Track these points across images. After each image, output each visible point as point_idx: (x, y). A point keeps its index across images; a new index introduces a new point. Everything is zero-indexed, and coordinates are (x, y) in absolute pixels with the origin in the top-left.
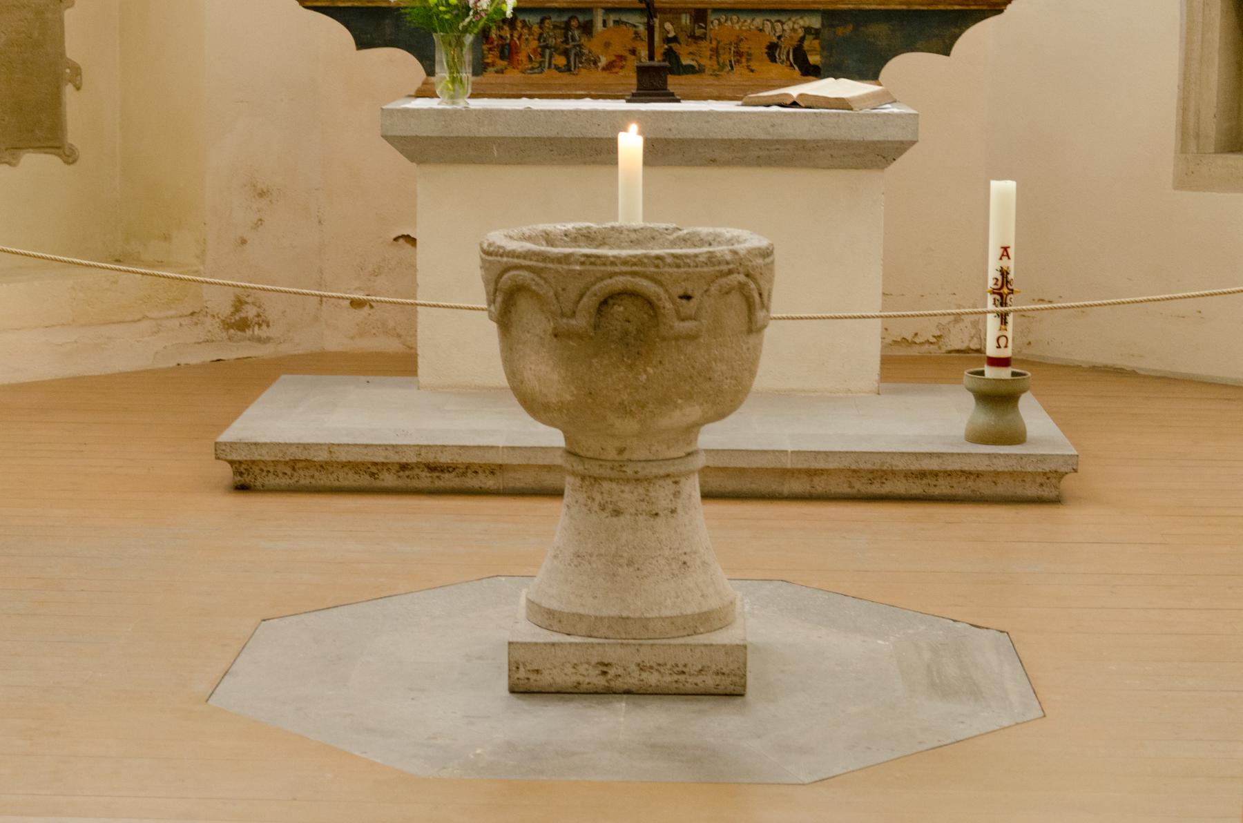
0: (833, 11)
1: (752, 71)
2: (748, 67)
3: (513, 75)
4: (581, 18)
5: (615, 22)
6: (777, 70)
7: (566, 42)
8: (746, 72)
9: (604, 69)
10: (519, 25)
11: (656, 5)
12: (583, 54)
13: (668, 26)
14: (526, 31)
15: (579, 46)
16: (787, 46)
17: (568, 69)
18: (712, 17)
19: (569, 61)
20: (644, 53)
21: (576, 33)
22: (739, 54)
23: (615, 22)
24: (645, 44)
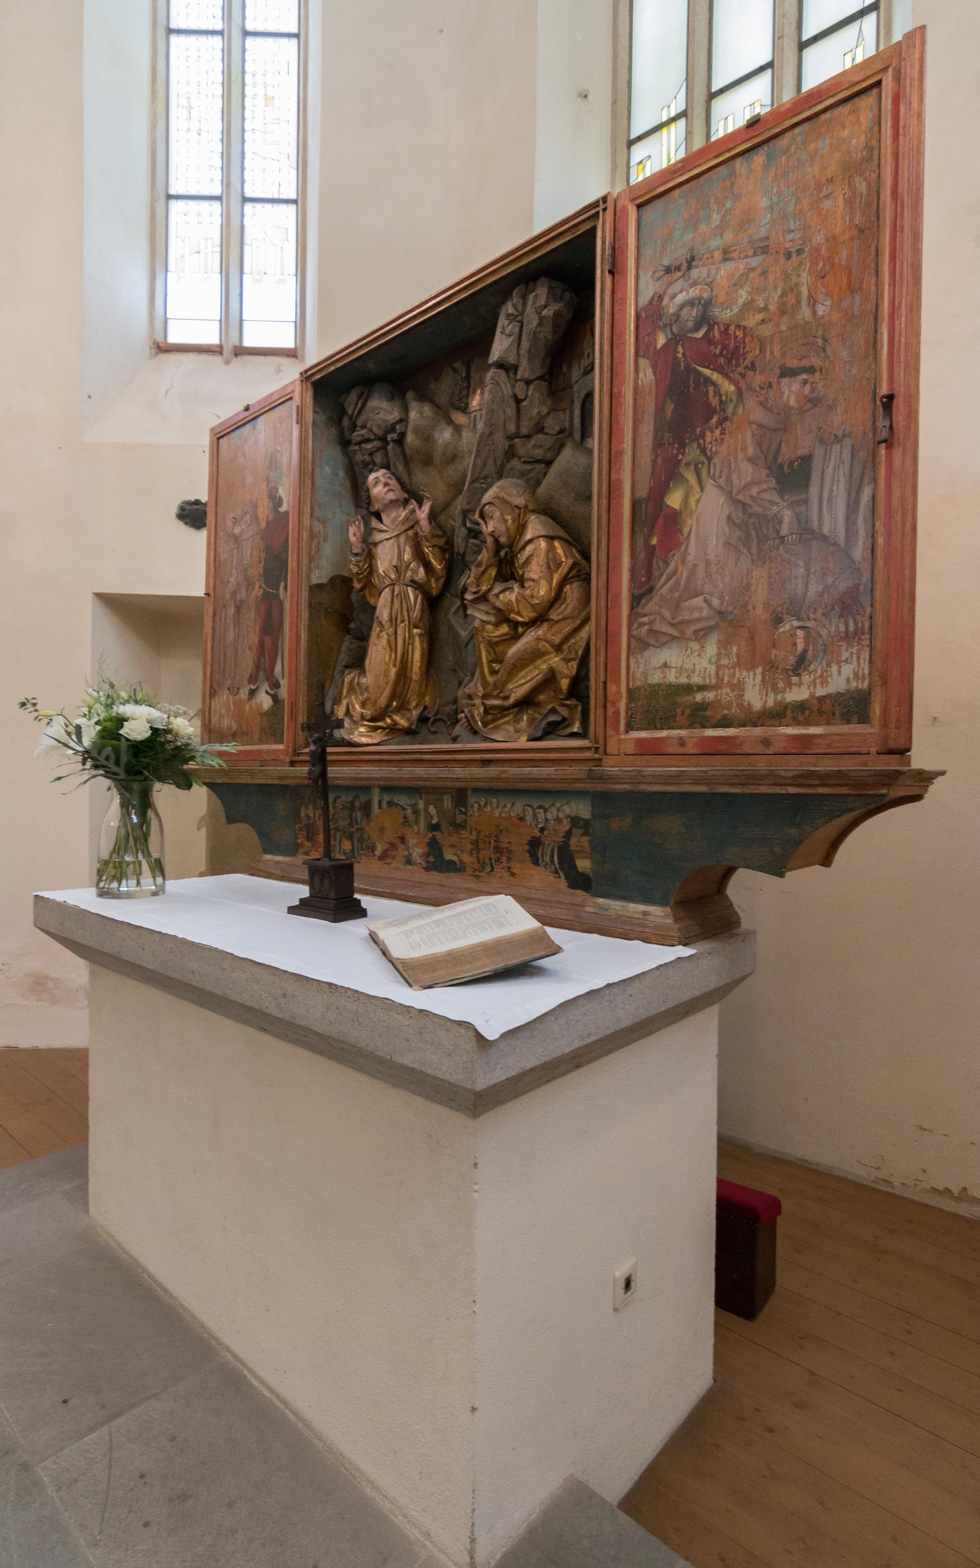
1: (513, 875)
2: (509, 868)
4: (363, 798)
5: (389, 802)
8: (505, 874)
16: (551, 841)
18: (472, 800)
22: (498, 850)
23: (389, 802)
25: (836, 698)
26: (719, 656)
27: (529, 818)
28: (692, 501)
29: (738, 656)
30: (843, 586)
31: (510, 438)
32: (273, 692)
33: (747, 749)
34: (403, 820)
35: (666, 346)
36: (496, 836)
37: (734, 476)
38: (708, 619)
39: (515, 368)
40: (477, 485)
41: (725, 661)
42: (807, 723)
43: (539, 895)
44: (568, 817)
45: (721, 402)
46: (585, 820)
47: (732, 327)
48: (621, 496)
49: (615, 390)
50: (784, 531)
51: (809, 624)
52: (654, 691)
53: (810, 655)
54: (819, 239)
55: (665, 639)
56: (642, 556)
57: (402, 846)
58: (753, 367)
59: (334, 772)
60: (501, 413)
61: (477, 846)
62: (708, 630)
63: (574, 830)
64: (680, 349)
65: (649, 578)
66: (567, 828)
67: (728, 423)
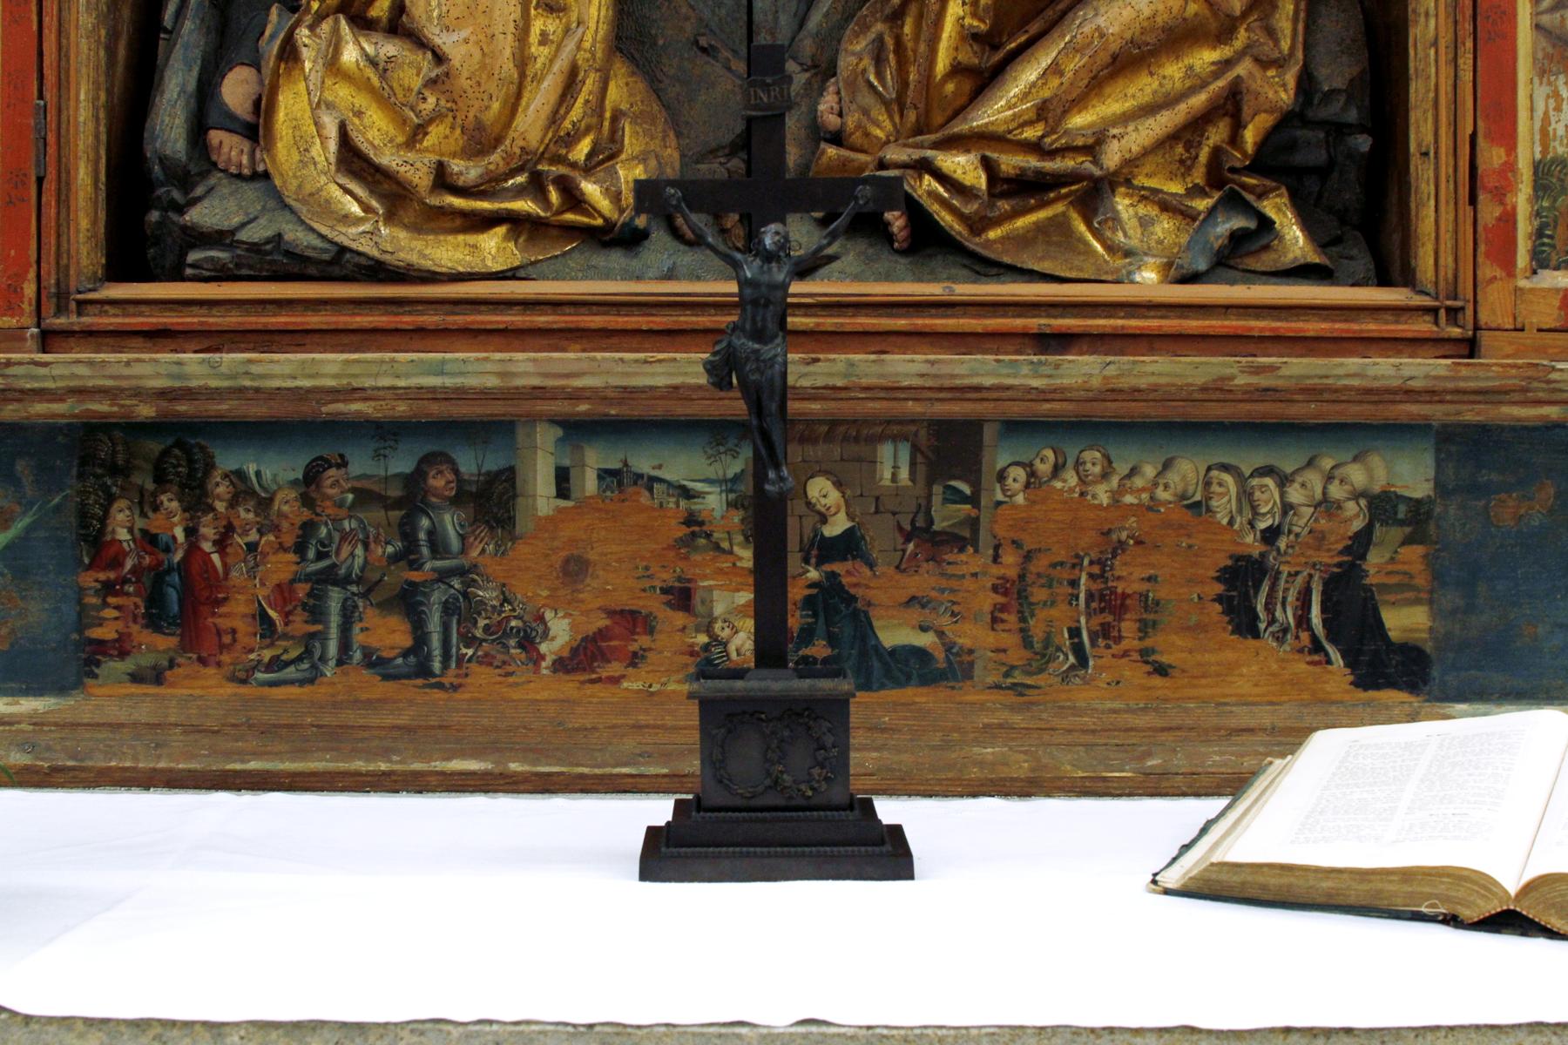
0: (1483, 429)
1: (1161, 670)
2: (1145, 653)
3: (203, 691)
4: (470, 462)
5: (604, 474)
6: (1255, 669)
7: (408, 556)
8: (1134, 673)
10: (221, 490)
12: (478, 607)
13: (821, 490)
14: (246, 514)
15: (461, 572)
18: (1000, 455)
19: (421, 639)
21: (450, 523)
22: (1109, 603)
23: (604, 474)
27: (1224, 503)
34: (685, 530)
36: (1101, 563)
44: (1356, 495)
46: (1418, 502)
57: (680, 618)
59: (806, 371)
61: (1022, 595)
63: (1378, 531)
66: (1358, 525)
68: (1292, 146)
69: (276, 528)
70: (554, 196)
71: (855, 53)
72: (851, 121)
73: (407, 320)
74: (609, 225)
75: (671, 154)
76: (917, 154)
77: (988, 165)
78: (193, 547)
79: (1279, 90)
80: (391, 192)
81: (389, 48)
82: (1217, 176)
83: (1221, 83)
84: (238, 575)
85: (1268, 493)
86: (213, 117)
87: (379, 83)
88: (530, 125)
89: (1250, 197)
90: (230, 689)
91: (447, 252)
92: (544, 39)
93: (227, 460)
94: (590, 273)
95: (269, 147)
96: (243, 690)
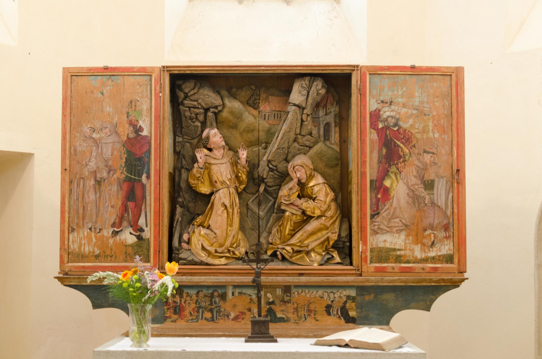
1: (317, 320)
3: (181, 323)
4: (220, 291)
5: (239, 293)
6: (332, 320)
9: (233, 320)
10: (185, 295)
11: (262, 284)
13: (269, 295)
14: (188, 298)
15: (219, 306)
16: (337, 306)
17: (212, 319)
18: (294, 290)
20: (255, 311)
22: (309, 311)
23: (239, 293)
24: (256, 305)
25: (444, 256)
26: (405, 239)
28: (394, 185)
29: (412, 240)
30: (445, 222)
31: (297, 135)
32: (138, 234)
33: (417, 271)
35: (382, 128)
37: (409, 181)
38: (401, 227)
39: (304, 109)
40: (278, 151)
41: (407, 241)
42: (435, 263)
43: (332, 327)
45: (404, 155)
47: (407, 131)
48: (366, 177)
49: (362, 138)
50: (426, 202)
51: (435, 232)
52: (380, 250)
53: (436, 242)
54: (435, 113)
55: (385, 232)
56: (374, 200)
57: (249, 313)
58: (414, 146)
60: (295, 124)
61: (297, 310)
62: (401, 230)
63: (348, 301)
64: (388, 131)
65: (378, 209)
66: (345, 300)
67: (406, 162)
68: (338, 244)
69: (192, 300)
70: (232, 253)
71: (274, 230)
72: (274, 241)
73: (211, 271)
74: (239, 257)
75: (248, 246)
76: (283, 247)
77: (292, 249)
78: (181, 303)
79: (335, 237)
80: (209, 253)
81: (208, 232)
82: (326, 249)
83: (326, 237)
84: (187, 307)
85: (332, 295)
86: (182, 241)
87: (206, 236)
88: (228, 243)
89: (330, 253)
90: (185, 323)
91: (217, 261)
92: (230, 230)
93: (186, 291)
94: (237, 264)
95: (191, 246)
96: (188, 323)
